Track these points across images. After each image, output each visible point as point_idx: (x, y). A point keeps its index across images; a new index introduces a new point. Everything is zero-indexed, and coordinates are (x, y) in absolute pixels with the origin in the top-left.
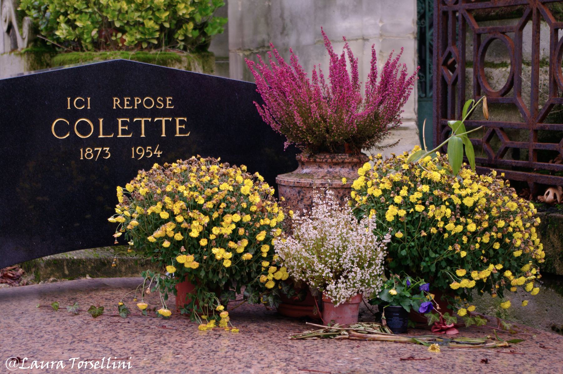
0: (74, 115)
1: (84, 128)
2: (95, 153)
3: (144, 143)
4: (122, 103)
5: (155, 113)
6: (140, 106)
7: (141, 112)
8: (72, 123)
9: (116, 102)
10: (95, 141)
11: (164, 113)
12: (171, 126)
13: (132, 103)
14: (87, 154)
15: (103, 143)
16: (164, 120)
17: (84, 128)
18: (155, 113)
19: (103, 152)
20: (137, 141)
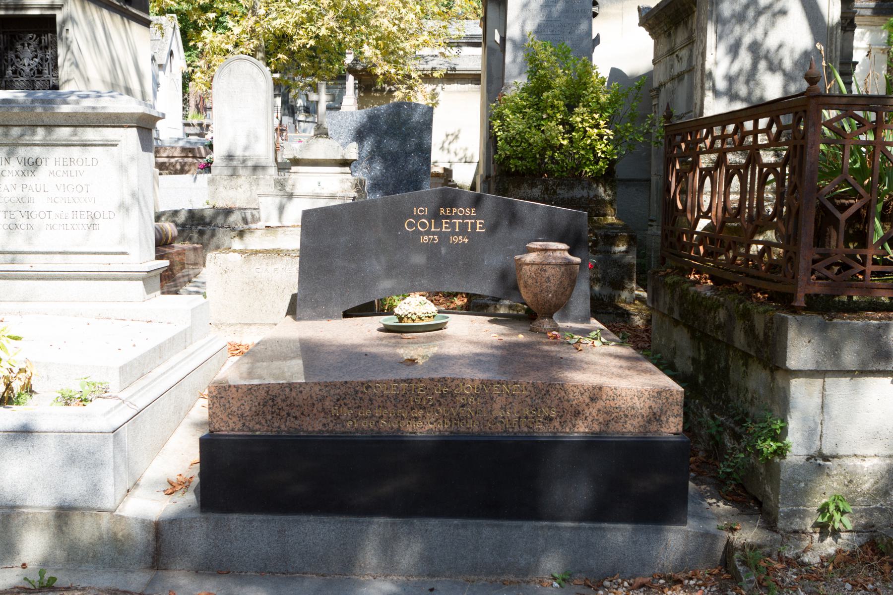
0: (417, 218)
1: (423, 225)
2: (429, 239)
3: (458, 234)
4: (445, 212)
5: (464, 217)
6: (456, 213)
7: (458, 217)
8: (417, 222)
9: (442, 211)
10: (428, 233)
11: (470, 217)
12: (474, 226)
13: (451, 211)
14: (425, 239)
15: (434, 233)
16: (469, 221)
17: (423, 225)
18: (464, 217)
19: (434, 239)
20: (453, 233)
